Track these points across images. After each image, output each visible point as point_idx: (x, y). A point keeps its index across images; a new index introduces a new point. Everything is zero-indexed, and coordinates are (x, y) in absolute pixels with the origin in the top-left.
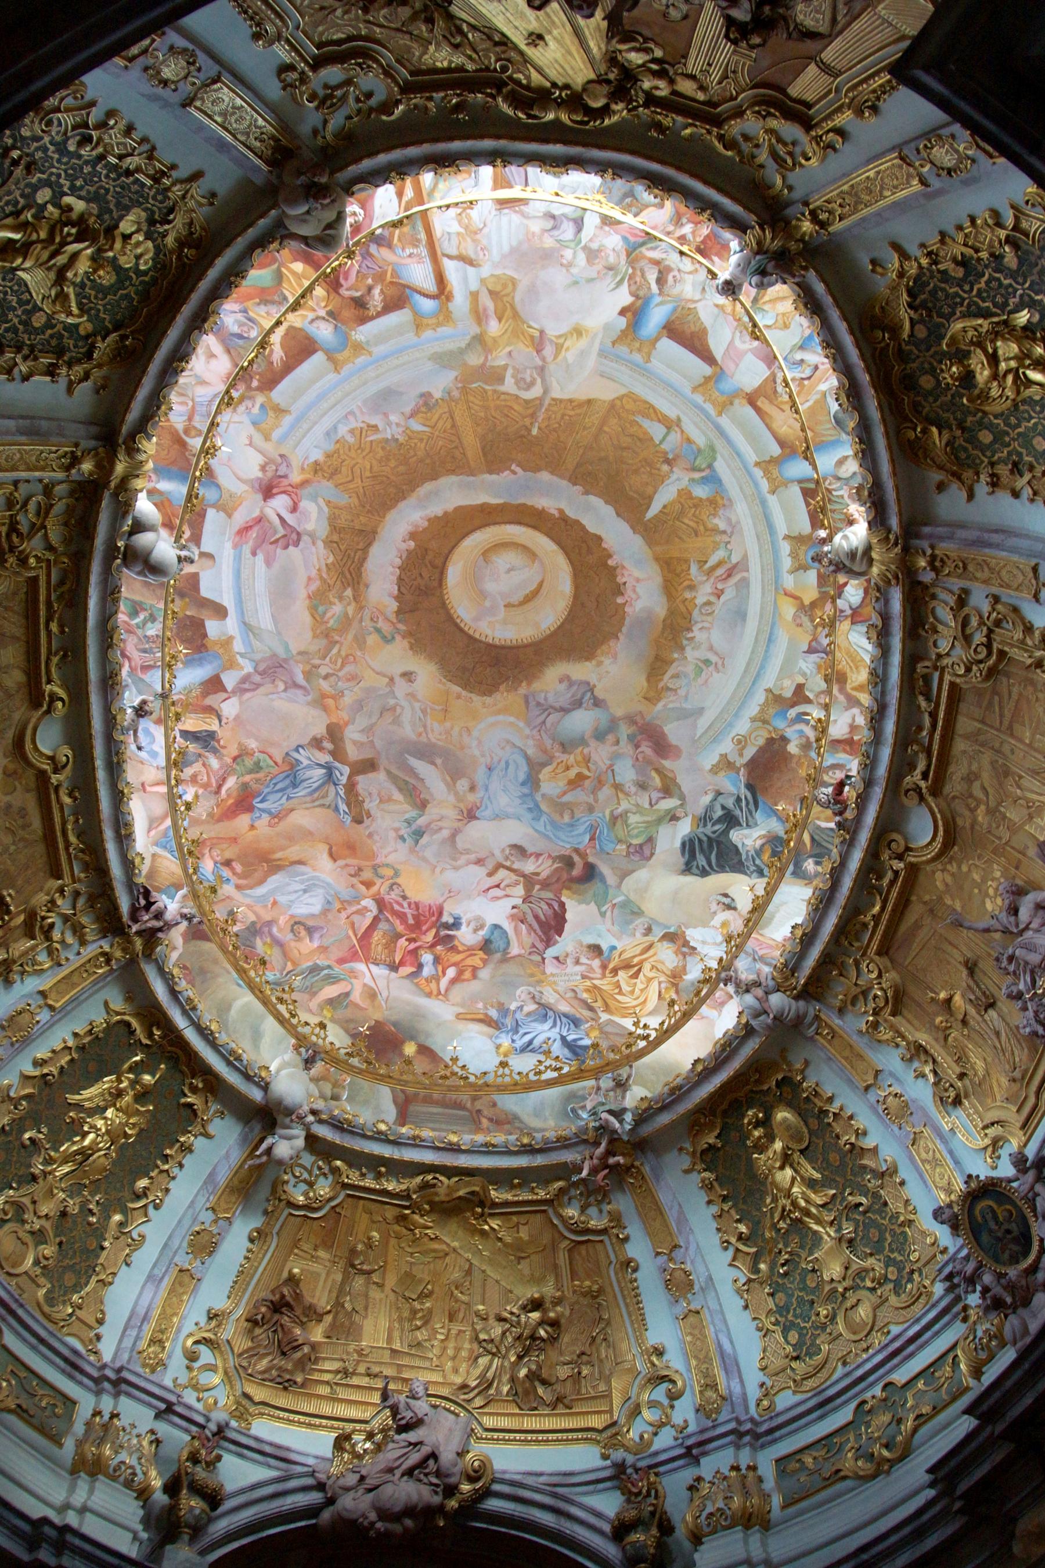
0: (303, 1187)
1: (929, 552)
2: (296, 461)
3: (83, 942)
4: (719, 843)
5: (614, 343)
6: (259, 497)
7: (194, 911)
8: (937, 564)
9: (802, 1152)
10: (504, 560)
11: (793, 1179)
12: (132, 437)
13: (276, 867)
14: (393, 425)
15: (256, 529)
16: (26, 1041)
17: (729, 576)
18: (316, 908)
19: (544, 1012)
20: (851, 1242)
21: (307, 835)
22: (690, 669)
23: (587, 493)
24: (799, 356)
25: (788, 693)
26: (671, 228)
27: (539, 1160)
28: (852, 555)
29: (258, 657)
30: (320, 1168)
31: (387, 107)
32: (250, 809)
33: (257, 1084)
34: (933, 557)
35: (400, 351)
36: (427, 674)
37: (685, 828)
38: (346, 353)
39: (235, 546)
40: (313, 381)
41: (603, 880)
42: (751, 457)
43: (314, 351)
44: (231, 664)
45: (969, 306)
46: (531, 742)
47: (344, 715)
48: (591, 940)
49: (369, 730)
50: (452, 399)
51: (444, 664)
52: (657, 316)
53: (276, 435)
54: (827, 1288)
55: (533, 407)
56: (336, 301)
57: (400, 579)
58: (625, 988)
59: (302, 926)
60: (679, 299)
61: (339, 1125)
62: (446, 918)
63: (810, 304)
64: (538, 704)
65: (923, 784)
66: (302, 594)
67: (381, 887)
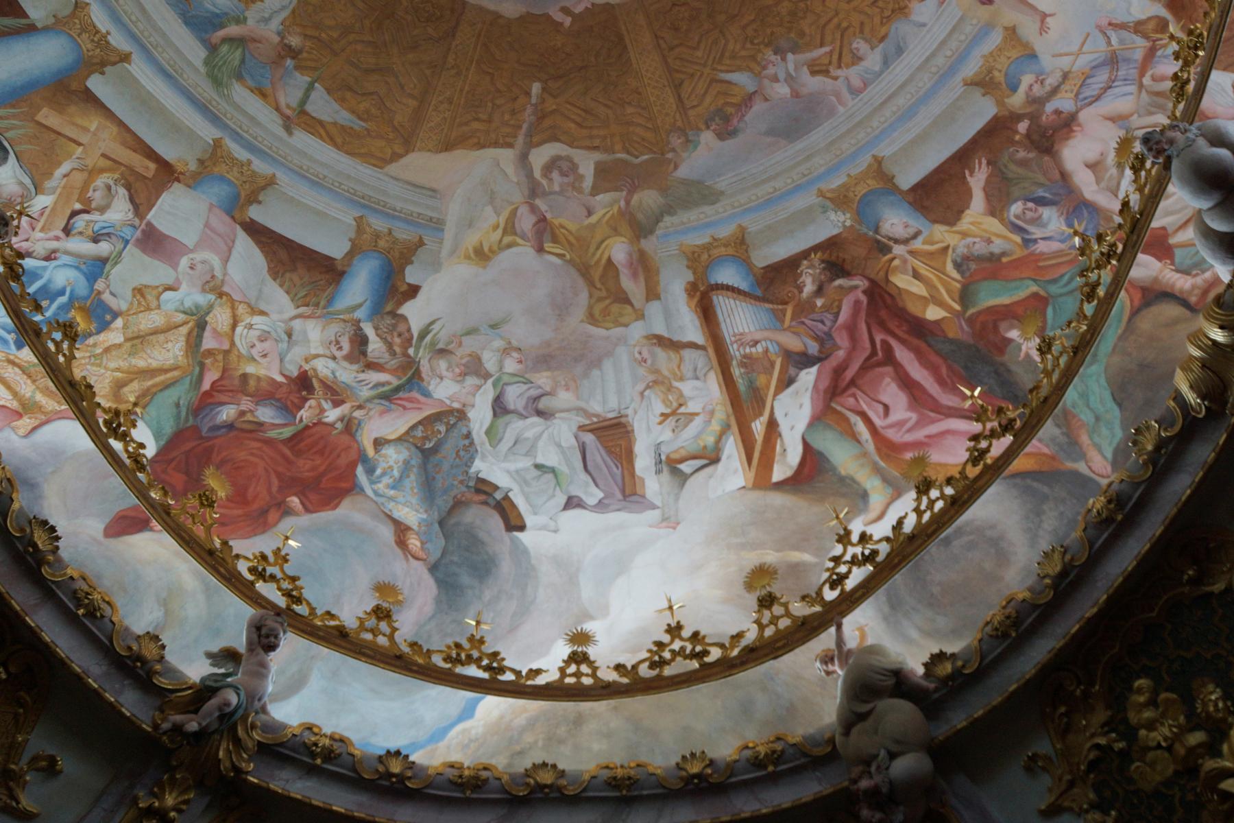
5: (421, 243)
14: (784, 77)
24: (104, 248)
26: (357, 414)
35: (769, 202)
38: (861, 190)
42: (139, 68)
43: (915, 188)
50: (682, 131)
52: (357, 289)
53: (995, 39)
55: (543, 131)
56: (875, 267)
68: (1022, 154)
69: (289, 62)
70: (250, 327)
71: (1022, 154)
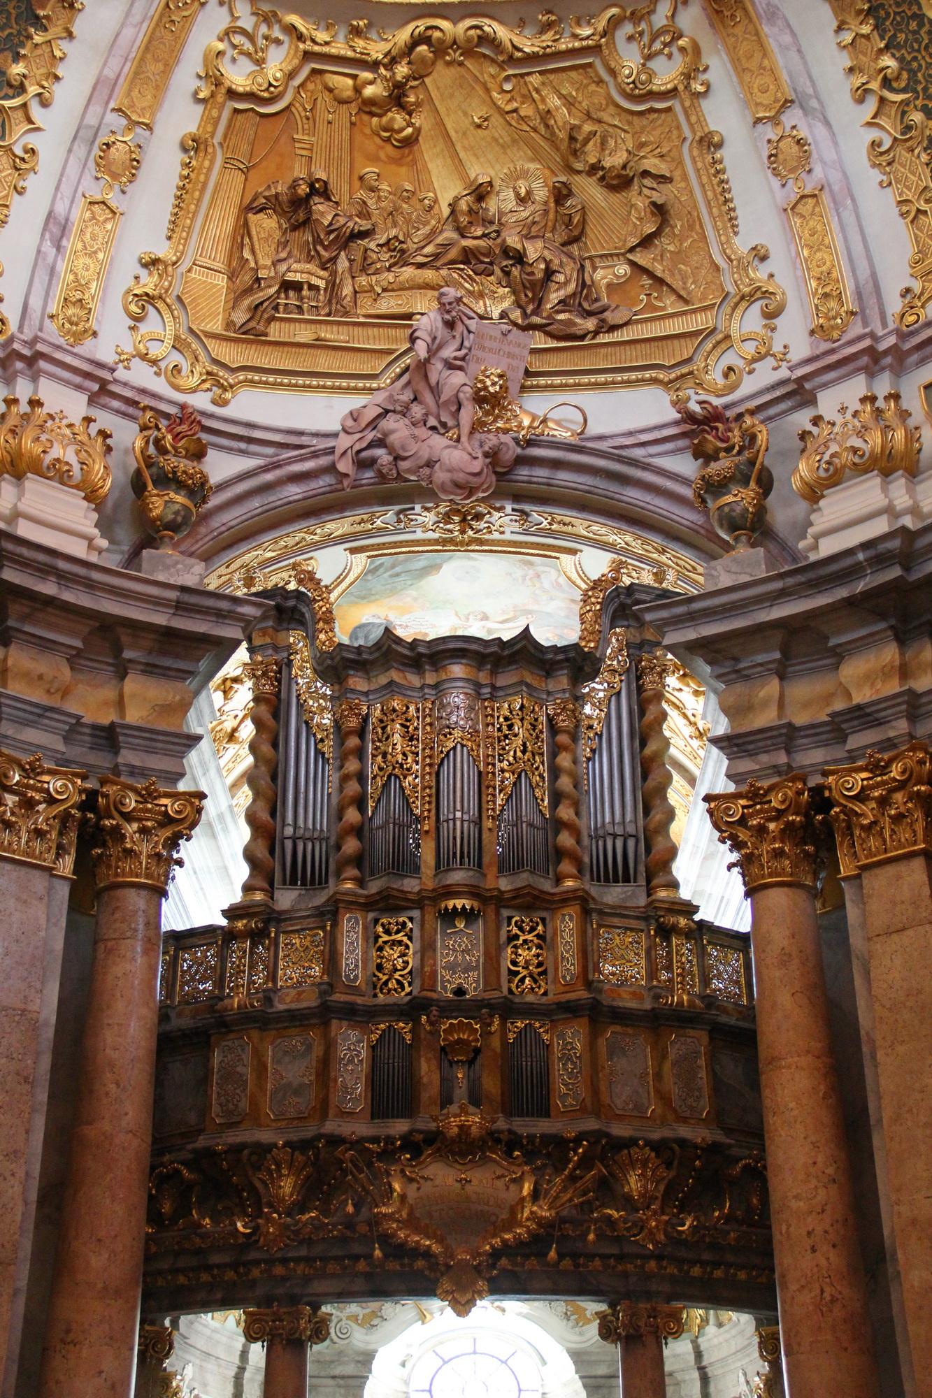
31: (615, 23)
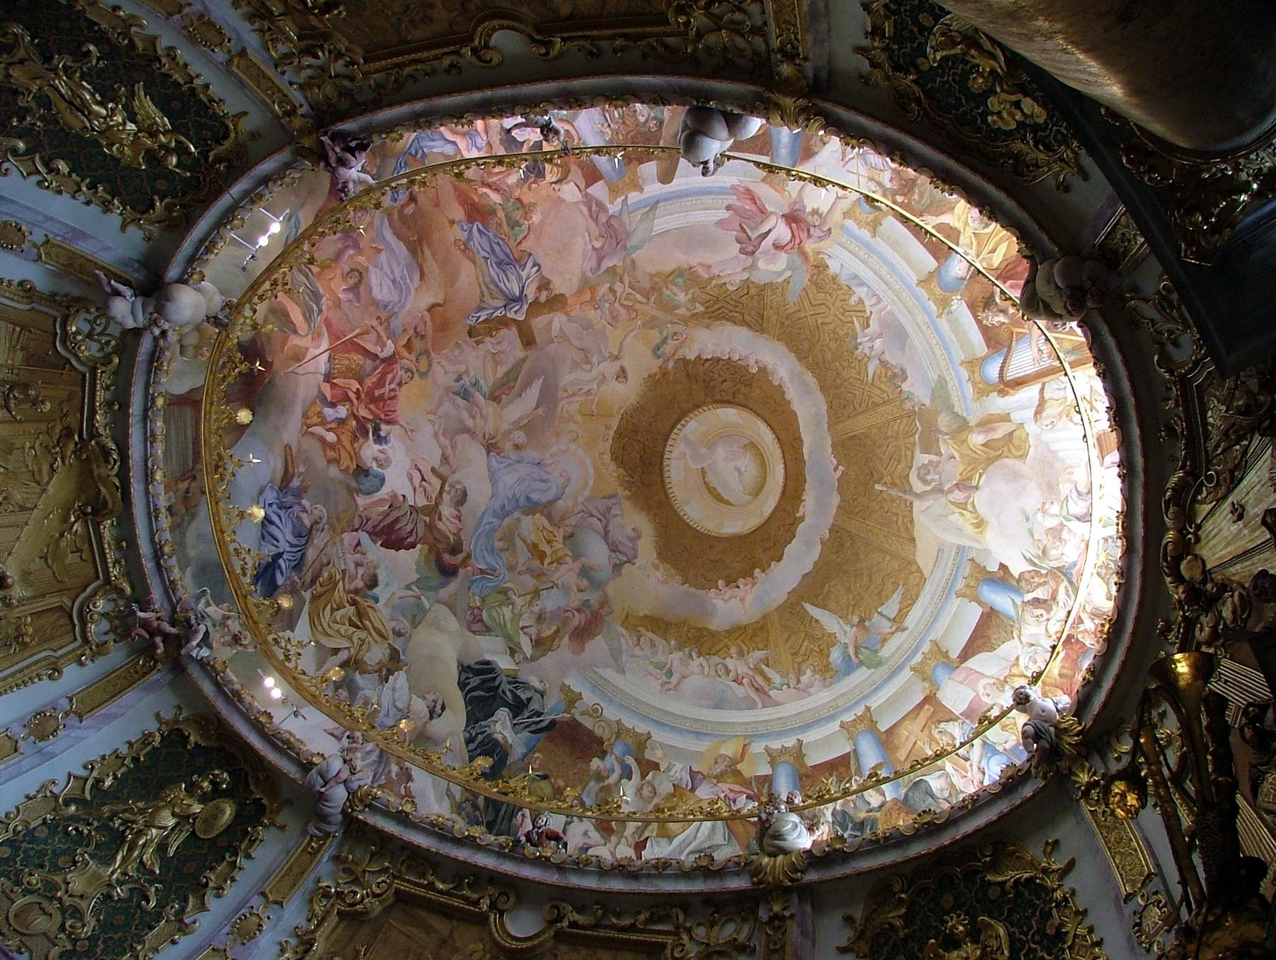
0: (86, 328)
1: (787, 914)
2: (828, 246)
3: (302, 87)
4: (494, 698)
5: (972, 560)
6: (787, 212)
7: (351, 194)
8: (776, 923)
9: (193, 833)
10: (747, 463)
11: (165, 828)
12: (820, 113)
13: (415, 248)
14: (871, 343)
15: (754, 208)
16: (192, 39)
17: (757, 690)
18: (378, 294)
19: (304, 535)
20: (108, 897)
21: (451, 278)
22: (661, 657)
23: (823, 543)
25: (648, 755)
27: (148, 565)
28: (779, 836)
29: (625, 217)
30: (108, 343)
31: (1166, 361)
32: (471, 220)
33: (184, 272)
34: (782, 919)
36: (626, 394)
37: (504, 663)
38: (938, 291)
39: (733, 187)
40: (906, 258)
41: (443, 585)
42: (874, 703)
43: (937, 259)
44: (614, 191)
45: (1020, 940)
46: (570, 503)
47: (576, 312)
48: (382, 577)
49: (563, 336)
50: (902, 401)
51: (640, 409)
52: (1002, 601)
53: (850, 223)
54: (58, 879)
57: (719, 360)
58: (338, 614)
59: (358, 279)
60: (1020, 620)
61: (155, 356)
62: (384, 429)
63: (1011, 782)
64: (609, 509)
65: (565, 923)
66: (694, 259)
67: (408, 360)
68: (916, 197)
69: (867, 623)
70: (1027, 667)
71: (916, 197)
